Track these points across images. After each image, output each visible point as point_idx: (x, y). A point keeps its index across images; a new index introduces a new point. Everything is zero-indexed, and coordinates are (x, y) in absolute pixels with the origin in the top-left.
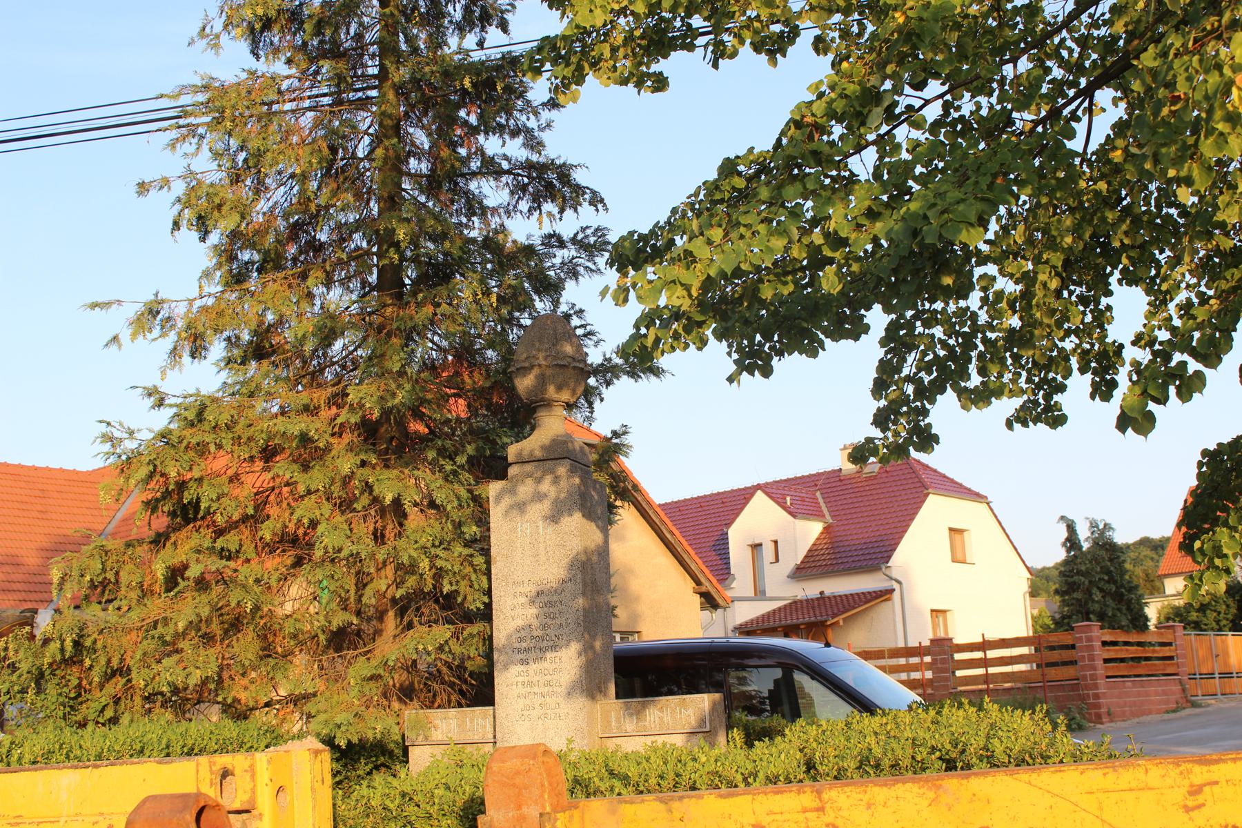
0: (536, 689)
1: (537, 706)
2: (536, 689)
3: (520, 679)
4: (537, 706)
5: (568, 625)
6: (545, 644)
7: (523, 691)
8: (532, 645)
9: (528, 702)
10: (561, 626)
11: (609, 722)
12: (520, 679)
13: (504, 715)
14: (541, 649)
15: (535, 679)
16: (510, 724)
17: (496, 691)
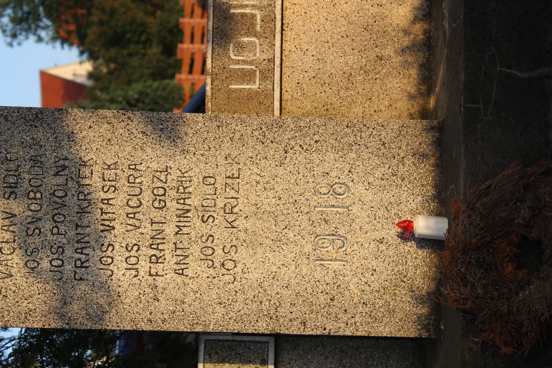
0: (170, 229)
1: (205, 229)
2: (170, 229)
3: (144, 266)
4: (205, 229)
5: (36, 143)
6: (72, 201)
7: (171, 260)
8: (72, 233)
9: (195, 250)
10: (36, 161)
11: (251, 96)
12: (144, 266)
13: (220, 310)
14: (82, 212)
15: (147, 229)
16: (240, 297)
17: (166, 327)
